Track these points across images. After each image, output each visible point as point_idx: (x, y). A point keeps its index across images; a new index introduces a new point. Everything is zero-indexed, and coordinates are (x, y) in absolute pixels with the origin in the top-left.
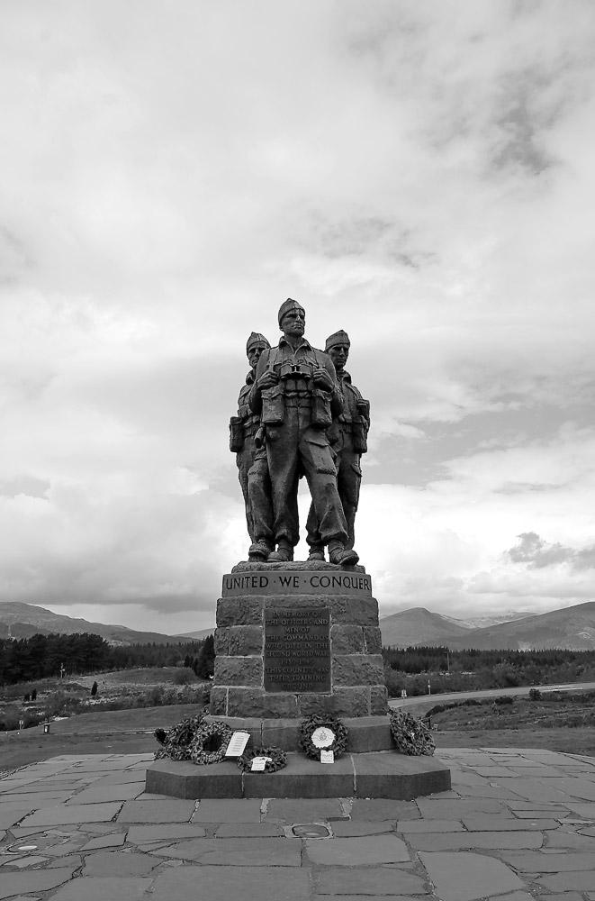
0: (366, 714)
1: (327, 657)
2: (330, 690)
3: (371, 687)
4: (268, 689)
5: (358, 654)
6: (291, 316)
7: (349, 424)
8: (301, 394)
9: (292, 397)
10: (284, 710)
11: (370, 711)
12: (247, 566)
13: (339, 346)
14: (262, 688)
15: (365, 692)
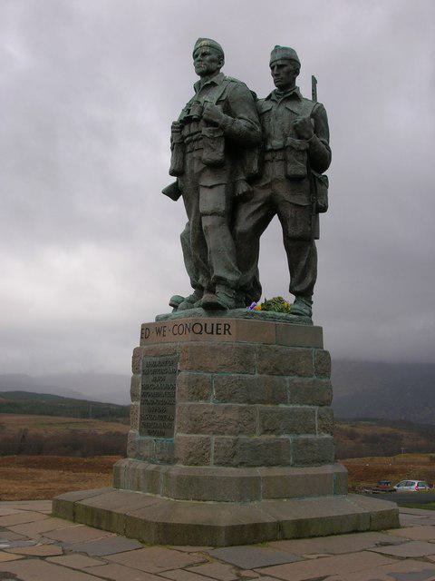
0: (206, 462)
1: (173, 404)
2: (172, 435)
3: (214, 438)
4: (140, 431)
5: (201, 402)
6: (209, 60)
7: (280, 150)
8: (194, 137)
9: (189, 142)
10: (146, 453)
11: (212, 460)
12: (166, 317)
13: (285, 67)
14: (137, 433)
15: (207, 442)
